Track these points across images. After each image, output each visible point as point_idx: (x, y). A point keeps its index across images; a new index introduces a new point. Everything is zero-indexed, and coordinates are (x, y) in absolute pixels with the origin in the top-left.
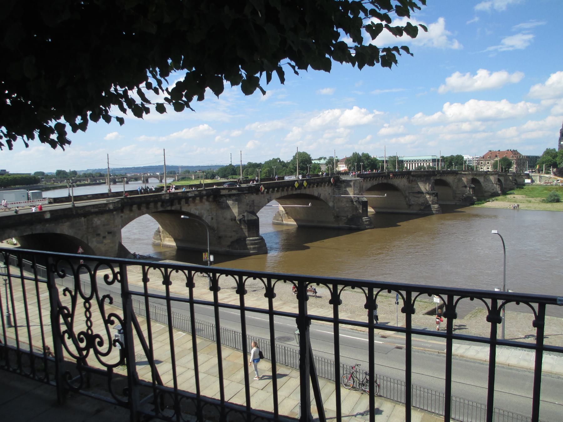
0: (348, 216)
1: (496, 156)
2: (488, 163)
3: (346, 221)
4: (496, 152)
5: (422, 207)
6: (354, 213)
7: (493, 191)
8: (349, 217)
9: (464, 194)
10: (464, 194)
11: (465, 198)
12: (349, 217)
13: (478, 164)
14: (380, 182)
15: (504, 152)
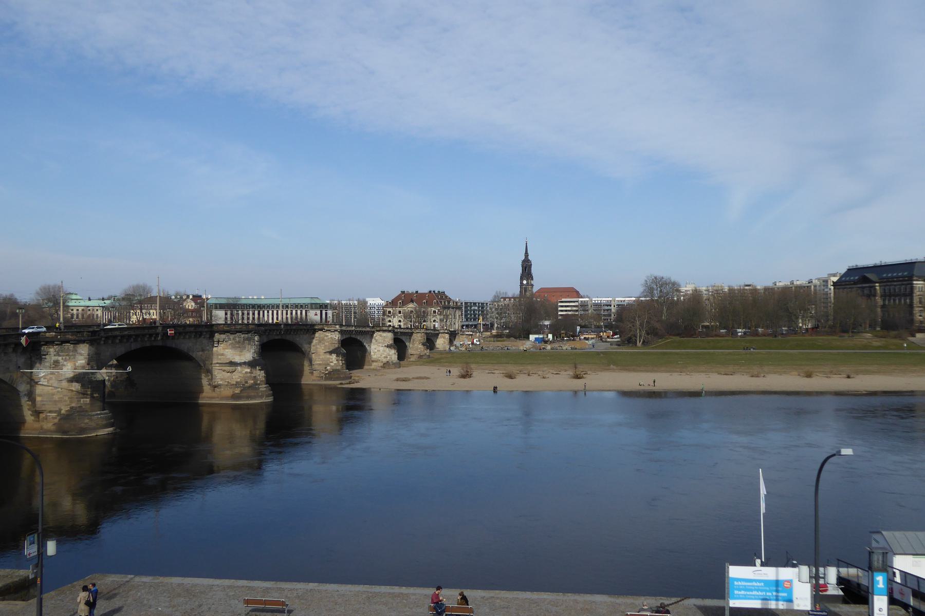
0: (60, 410)
1: (412, 301)
2: (400, 312)
3: (56, 421)
4: (412, 294)
5: (237, 391)
6: (73, 405)
7: (385, 360)
8: (63, 412)
9: (328, 365)
10: (328, 365)
11: (330, 373)
12: (63, 412)
13: (384, 314)
14: (148, 344)
15: (425, 294)
